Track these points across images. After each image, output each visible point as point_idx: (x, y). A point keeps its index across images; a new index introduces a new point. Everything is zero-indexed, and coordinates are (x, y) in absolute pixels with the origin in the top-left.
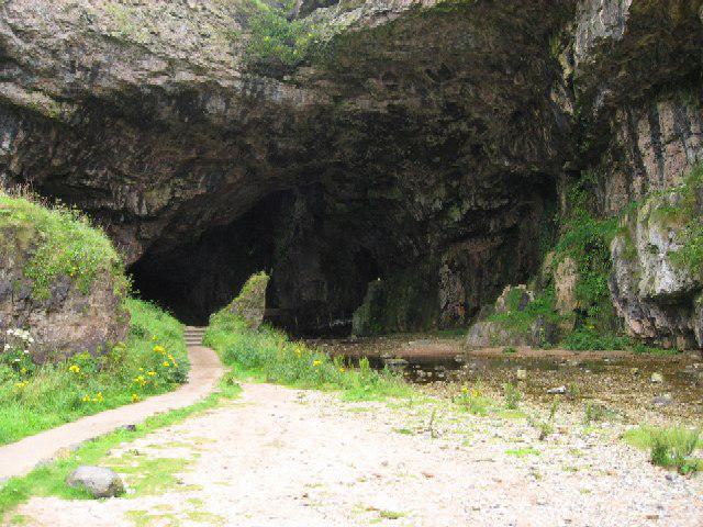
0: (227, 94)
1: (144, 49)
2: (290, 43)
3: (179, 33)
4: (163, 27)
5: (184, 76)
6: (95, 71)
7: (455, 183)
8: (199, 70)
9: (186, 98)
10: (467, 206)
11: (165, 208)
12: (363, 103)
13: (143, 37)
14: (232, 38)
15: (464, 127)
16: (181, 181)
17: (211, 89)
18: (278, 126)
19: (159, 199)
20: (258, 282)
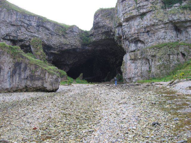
0: (79, 49)
1: (68, 45)
2: (88, 41)
3: (73, 42)
4: (70, 42)
5: (73, 47)
6: (62, 48)
7: (116, 57)
8: (75, 46)
9: (74, 50)
10: (119, 61)
11: (72, 63)
12: (98, 49)
13: (68, 43)
14: (80, 41)
15: (114, 51)
16: (74, 59)
17: (77, 48)
18: (87, 51)
19: (71, 62)
20: (82, 74)
